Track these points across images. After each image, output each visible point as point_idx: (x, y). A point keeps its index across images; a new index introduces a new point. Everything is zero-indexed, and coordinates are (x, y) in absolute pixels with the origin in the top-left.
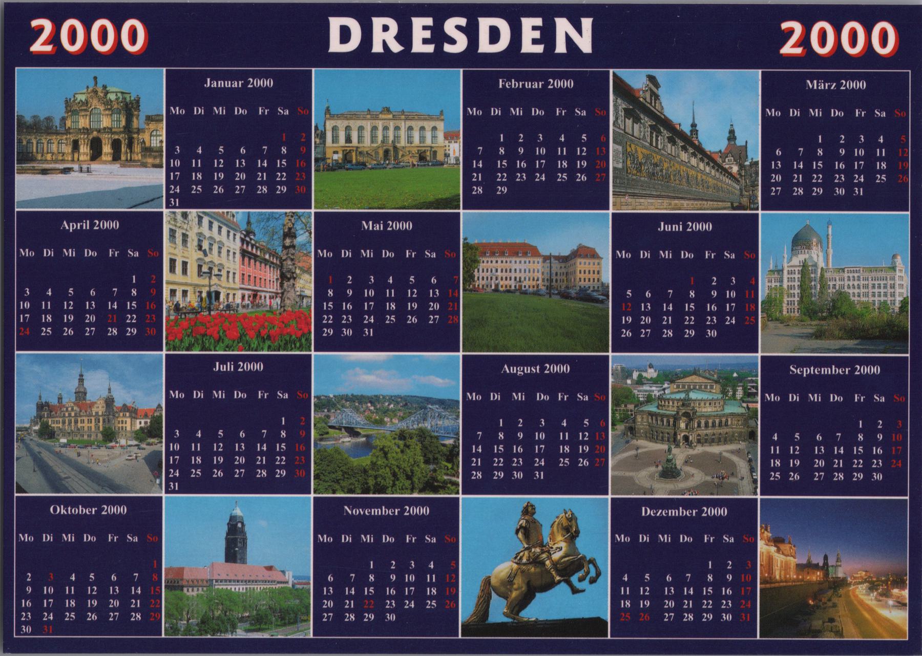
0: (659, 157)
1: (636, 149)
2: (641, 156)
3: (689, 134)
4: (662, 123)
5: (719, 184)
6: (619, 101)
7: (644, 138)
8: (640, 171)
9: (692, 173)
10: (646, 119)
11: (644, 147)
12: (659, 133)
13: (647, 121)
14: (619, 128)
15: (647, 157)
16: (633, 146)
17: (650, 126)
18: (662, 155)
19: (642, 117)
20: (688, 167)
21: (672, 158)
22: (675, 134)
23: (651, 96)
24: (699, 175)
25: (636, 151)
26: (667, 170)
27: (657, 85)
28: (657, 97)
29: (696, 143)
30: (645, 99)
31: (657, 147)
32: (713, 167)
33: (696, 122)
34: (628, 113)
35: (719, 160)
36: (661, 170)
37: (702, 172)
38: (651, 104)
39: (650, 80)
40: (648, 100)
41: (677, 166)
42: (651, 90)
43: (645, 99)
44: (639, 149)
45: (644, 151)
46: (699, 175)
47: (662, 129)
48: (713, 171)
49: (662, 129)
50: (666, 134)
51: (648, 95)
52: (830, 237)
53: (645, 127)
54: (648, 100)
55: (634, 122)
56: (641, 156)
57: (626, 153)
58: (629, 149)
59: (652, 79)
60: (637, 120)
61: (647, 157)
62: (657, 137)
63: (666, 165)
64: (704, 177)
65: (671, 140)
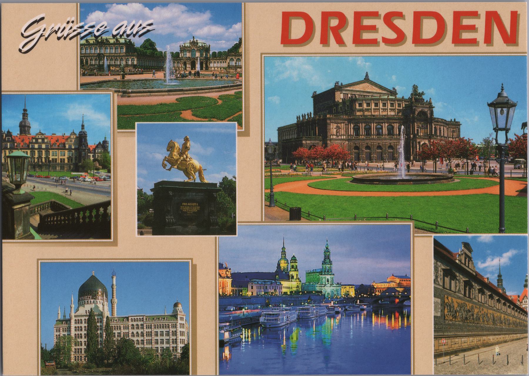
0: (471, 305)
1: (452, 300)
2: (456, 305)
3: (495, 284)
4: (474, 279)
5: (518, 320)
6: (439, 264)
7: (459, 291)
8: (455, 317)
9: (497, 314)
10: (461, 276)
11: (459, 298)
12: (471, 287)
13: (462, 278)
14: (439, 285)
15: (461, 306)
16: (450, 298)
17: (464, 281)
18: (473, 303)
19: (458, 274)
20: (494, 310)
21: (481, 305)
22: (485, 286)
23: (465, 259)
24: (503, 315)
25: (453, 302)
26: (477, 314)
27: (470, 251)
28: (470, 259)
29: (501, 291)
30: (460, 261)
31: (469, 297)
32: (513, 309)
33: (501, 274)
34: (446, 273)
35: (518, 303)
36: (473, 315)
37: (505, 313)
38: (465, 264)
39: (465, 247)
40: (463, 261)
41: (485, 310)
42: (465, 254)
43: (460, 261)
44: (454, 300)
45: (459, 301)
46: (503, 315)
47: (473, 284)
48: (513, 312)
49: (473, 284)
50: (477, 287)
51: (463, 258)
52: (115, 287)
53: (459, 282)
54: (463, 261)
55: (451, 279)
56: (456, 305)
57: (444, 304)
58: (446, 301)
59: (467, 245)
60: (453, 277)
61: (461, 306)
62: (470, 289)
63: (476, 311)
64: (506, 316)
65: (481, 291)
